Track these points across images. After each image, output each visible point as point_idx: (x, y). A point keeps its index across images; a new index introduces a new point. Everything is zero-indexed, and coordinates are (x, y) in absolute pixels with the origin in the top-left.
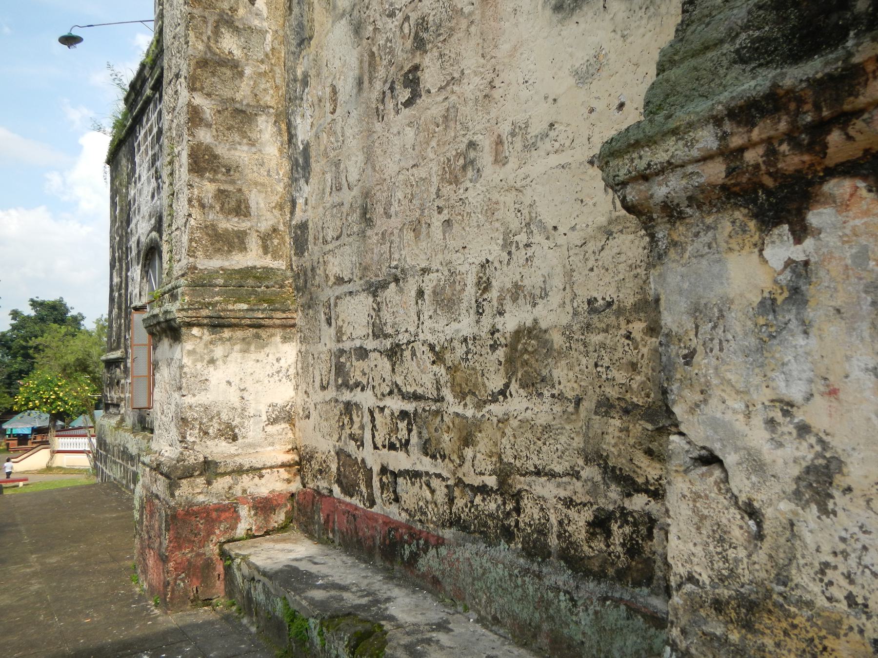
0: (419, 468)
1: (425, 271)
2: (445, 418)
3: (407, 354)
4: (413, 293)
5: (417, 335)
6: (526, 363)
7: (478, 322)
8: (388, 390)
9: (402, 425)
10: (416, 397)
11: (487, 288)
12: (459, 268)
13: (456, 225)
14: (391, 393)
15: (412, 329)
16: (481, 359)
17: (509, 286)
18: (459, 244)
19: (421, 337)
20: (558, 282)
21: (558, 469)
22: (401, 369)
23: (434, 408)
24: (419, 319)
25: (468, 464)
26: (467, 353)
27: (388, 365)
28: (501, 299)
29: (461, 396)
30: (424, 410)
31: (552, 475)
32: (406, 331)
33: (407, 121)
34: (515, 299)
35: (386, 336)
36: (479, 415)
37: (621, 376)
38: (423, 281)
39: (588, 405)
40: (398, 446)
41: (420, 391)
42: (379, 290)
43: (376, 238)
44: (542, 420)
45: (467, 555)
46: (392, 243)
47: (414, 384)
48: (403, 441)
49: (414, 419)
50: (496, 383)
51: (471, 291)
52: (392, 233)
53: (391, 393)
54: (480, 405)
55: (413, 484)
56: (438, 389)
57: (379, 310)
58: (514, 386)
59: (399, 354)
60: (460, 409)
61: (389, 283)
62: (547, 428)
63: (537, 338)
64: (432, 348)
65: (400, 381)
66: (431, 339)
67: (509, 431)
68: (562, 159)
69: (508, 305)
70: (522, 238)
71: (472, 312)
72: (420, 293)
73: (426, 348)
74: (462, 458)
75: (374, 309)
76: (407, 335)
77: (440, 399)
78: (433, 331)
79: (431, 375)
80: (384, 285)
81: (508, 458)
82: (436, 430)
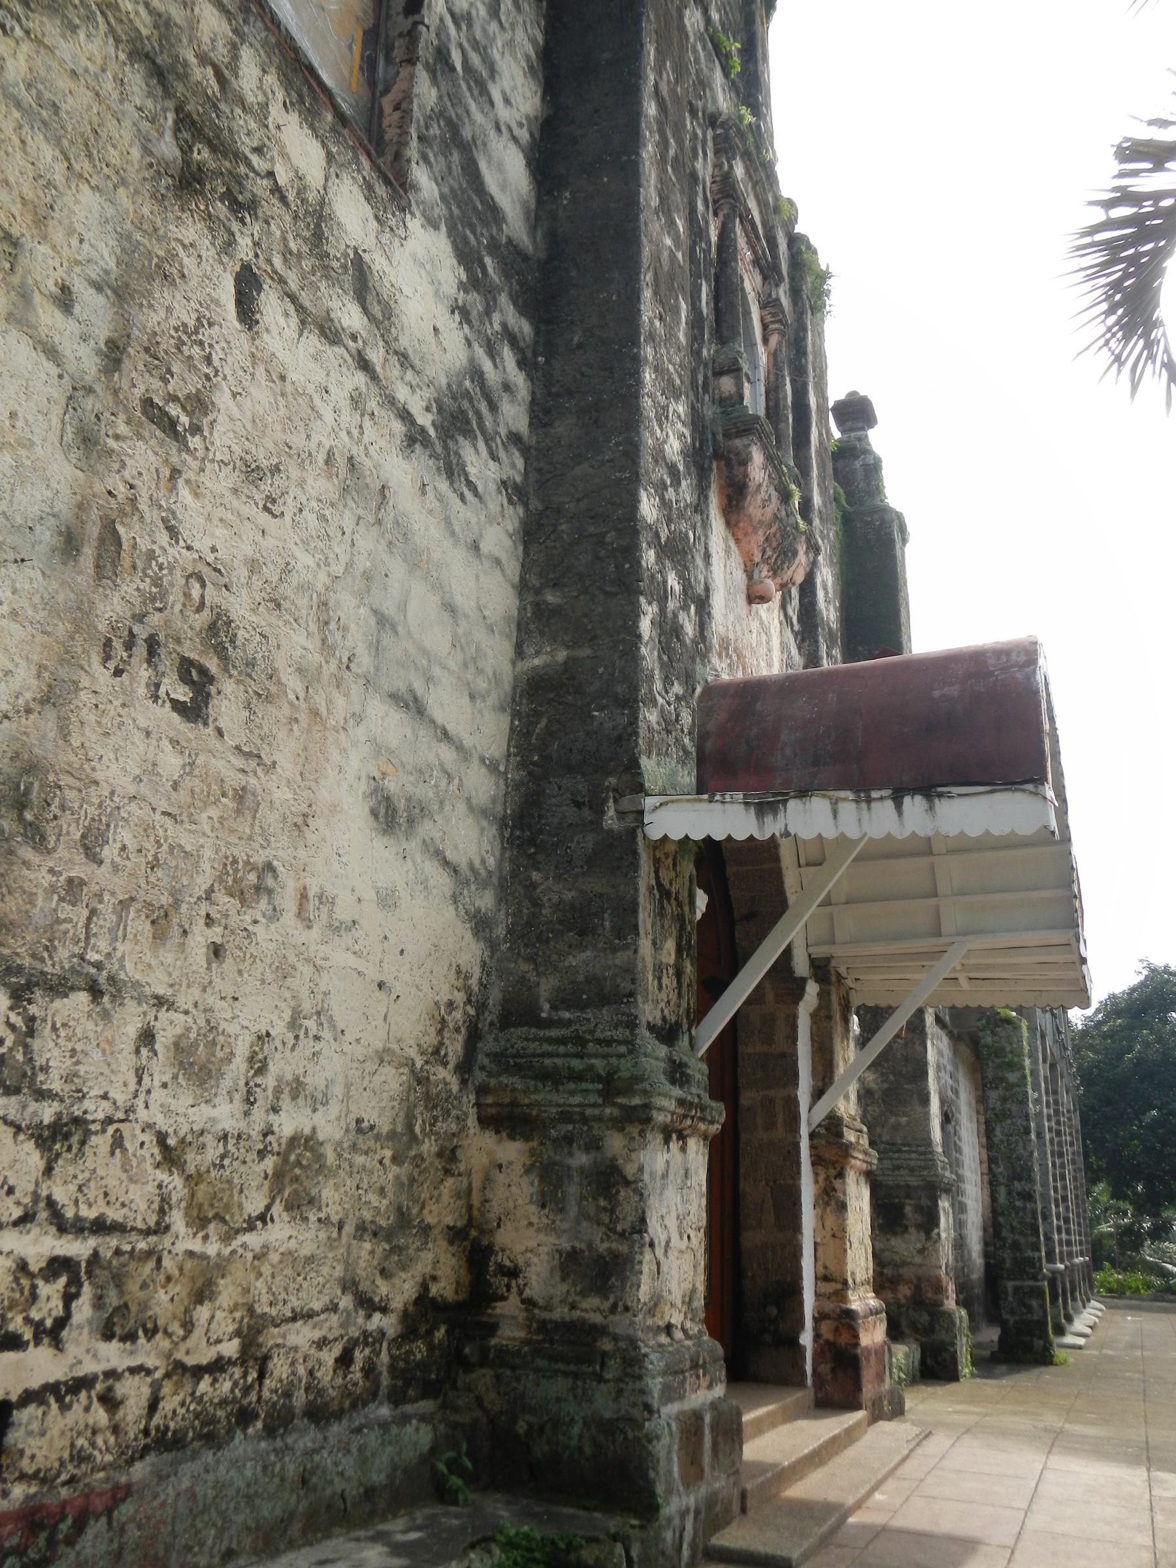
0: (90, 1367)
1: (160, 1002)
2: (167, 1262)
3: (101, 1142)
4: (132, 1030)
5: (130, 1110)
6: (296, 1179)
7: (247, 1114)
8: (17, 1213)
9: (51, 1292)
10: (100, 1227)
11: (262, 1070)
12: (224, 1025)
13: (229, 960)
14: (26, 1219)
15: (120, 1096)
16: (243, 1169)
17: (289, 1077)
18: (229, 991)
19: (142, 1114)
20: (338, 1090)
21: (317, 1306)
22: (71, 1170)
23: (142, 1245)
24: (139, 1082)
25: (198, 1333)
26: (223, 1157)
27: (34, 1159)
28: (278, 1091)
29: (199, 1221)
30: (118, 1252)
31: (309, 1315)
32: (105, 1097)
33: (172, 734)
34: (294, 1098)
35: (42, 1095)
36: (227, 1251)
37: (374, 1198)
38: (156, 1019)
39: (349, 1229)
40: (28, 1335)
41: (114, 1214)
42: (38, 993)
43: (49, 877)
44: (306, 1251)
45: (186, 1483)
46: (93, 912)
47: (101, 1202)
48: (49, 1323)
49: (89, 1273)
50: (254, 1204)
51: (239, 1067)
52: (99, 897)
53: (26, 1219)
54: (227, 1238)
55: (64, 1408)
56: (162, 1212)
57: (31, 1033)
58: (277, 1209)
59: (75, 1140)
60: (196, 1245)
61: (73, 989)
62: (310, 1259)
63: (312, 1150)
64: (161, 1138)
65: (61, 1194)
66: (162, 1124)
67: (266, 1270)
68: (360, 964)
69: (286, 1103)
70: (311, 1024)
71: (237, 1097)
72: (147, 1037)
73: (148, 1137)
74: (188, 1326)
75: (12, 1027)
76: (105, 1104)
77: (161, 1229)
78: (167, 1111)
79: (151, 1188)
80: (59, 988)
81: (262, 1308)
82: (144, 1286)
